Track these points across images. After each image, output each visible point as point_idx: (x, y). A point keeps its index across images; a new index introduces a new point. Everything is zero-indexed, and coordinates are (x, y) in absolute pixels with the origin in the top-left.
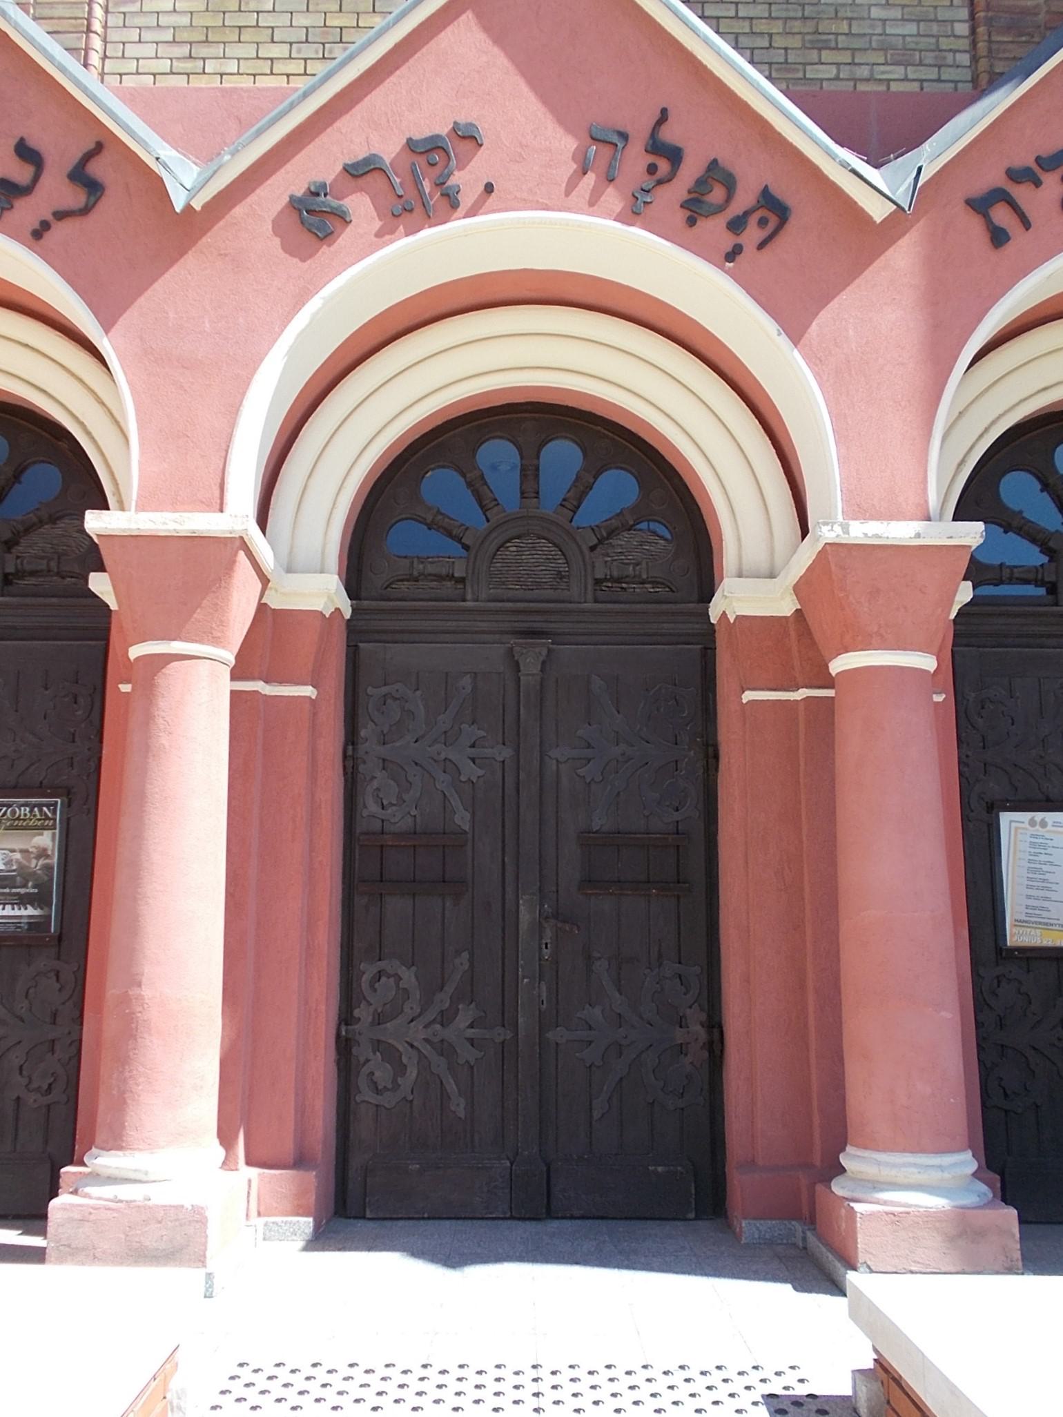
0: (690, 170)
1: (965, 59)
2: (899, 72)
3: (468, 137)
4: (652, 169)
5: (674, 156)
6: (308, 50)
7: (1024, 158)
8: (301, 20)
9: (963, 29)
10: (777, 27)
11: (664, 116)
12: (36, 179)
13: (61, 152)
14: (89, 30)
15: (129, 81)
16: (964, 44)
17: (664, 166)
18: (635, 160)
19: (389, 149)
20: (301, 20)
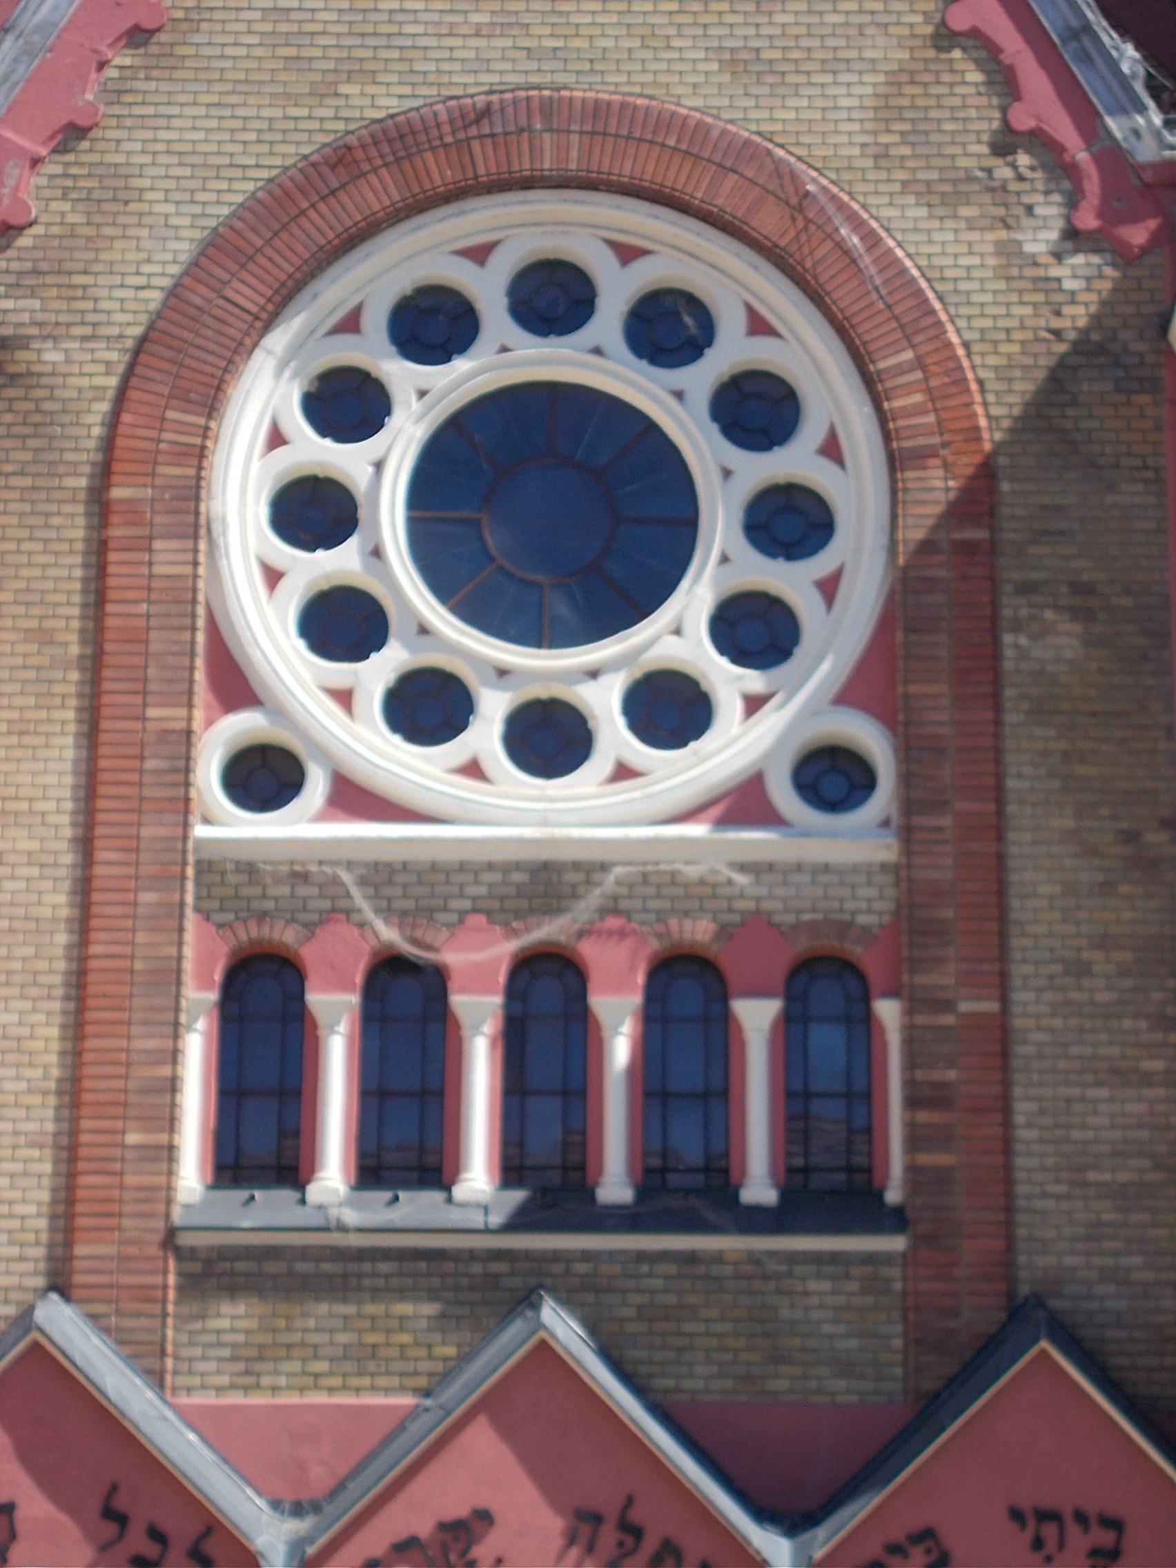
0: (650, 1545)
1: (898, 1371)
2: (842, 1384)
3: (484, 1517)
4: (621, 1544)
5: (637, 1533)
6: (349, 1366)
7: (897, 1534)
8: (343, 1338)
9: (898, 1343)
10: (742, 1343)
11: (629, 1501)
12: (162, 1555)
13: (182, 1532)
14: (163, 1353)
15: (198, 1399)
16: (899, 1357)
17: (629, 1541)
18: (609, 1536)
19: (423, 1528)
20: (343, 1338)
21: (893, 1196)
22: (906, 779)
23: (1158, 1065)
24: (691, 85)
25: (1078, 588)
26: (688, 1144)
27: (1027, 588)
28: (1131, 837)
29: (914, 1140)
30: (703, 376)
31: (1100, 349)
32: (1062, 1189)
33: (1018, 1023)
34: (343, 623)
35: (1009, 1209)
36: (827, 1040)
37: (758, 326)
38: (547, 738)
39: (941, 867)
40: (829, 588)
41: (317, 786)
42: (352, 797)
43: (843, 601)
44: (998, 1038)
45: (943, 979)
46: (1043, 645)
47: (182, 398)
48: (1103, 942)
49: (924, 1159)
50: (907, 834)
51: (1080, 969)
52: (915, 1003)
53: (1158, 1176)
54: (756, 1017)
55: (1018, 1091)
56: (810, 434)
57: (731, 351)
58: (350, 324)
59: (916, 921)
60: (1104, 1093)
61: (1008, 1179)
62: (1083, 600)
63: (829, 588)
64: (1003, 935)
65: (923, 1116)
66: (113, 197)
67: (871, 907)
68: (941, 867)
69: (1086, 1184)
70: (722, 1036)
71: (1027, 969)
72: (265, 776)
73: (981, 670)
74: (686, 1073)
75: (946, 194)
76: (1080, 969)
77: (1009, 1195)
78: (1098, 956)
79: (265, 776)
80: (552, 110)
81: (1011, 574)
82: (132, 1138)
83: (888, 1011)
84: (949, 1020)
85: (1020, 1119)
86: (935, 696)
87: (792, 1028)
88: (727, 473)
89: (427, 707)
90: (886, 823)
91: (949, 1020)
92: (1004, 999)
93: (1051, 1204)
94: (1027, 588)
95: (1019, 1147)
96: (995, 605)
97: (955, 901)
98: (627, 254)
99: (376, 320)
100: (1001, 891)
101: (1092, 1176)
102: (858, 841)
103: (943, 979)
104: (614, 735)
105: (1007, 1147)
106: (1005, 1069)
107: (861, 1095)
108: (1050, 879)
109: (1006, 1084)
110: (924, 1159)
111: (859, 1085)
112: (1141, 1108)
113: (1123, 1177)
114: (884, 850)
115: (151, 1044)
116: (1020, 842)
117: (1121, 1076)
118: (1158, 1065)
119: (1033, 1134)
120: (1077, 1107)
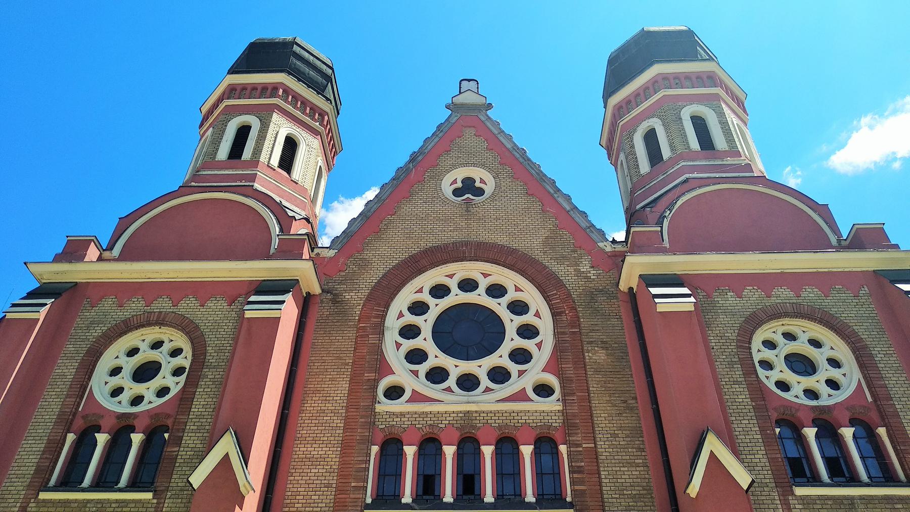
21: (569, 499)
22: (563, 387)
23: (641, 461)
24: (501, 239)
25: (605, 343)
26: (509, 489)
27: (591, 343)
28: (625, 402)
29: (573, 483)
30: (505, 300)
31: (602, 290)
32: (617, 496)
33: (600, 450)
34: (415, 357)
35: (603, 502)
36: (546, 459)
37: (517, 289)
38: (468, 383)
39: (575, 409)
40: (539, 346)
41: (407, 395)
42: (417, 397)
43: (542, 349)
44: (594, 454)
45: (578, 438)
46: (597, 356)
47: (379, 305)
48: (621, 428)
49: (577, 487)
50: (564, 401)
51: (615, 436)
52: (570, 445)
53: (645, 492)
54: (527, 451)
55: (602, 469)
56: (532, 311)
57: (511, 295)
58: (420, 291)
59: (569, 424)
60: (626, 469)
61: (602, 494)
62: (605, 345)
63: (539, 346)
64: (593, 427)
65: (575, 476)
66: (364, 265)
67: (557, 422)
68: (575, 409)
69: (624, 494)
70: (517, 455)
71: (601, 436)
72: (394, 392)
73: (580, 362)
74: (508, 469)
75: (561, 259)
76: (615, 436)
77: (602, 498)
78: (620, 432)
79: (394, 392)
80: (466, 244)
81: (584, 339)
82: (353, 484)
83: (563, 448)
84: (581, 449)
85: (603, 477)
86: (569, 369)
87: (537, 454)
88: (512, 321)
89: (437, 375)
90: (558, 400)
91: (581, 449)
92: (595, 443)
93: (614, 500)
94: (591, 343)
95: (604, 484)
96: (583, 347)
97: (577, 419)
98: (485, 275)
99: (426, 290)
100: (591, 416)
101: (625, 492)
102: (552, 405)
103: (578, 438)
104: (485, 382)
105: (600, 484)
106: (597, 462)
107: (557, 474)
108: (604, 415)
109: (598, 467)
110: (577, 487)
111: (556, 471)
112: (638, 473)
113: (634, 492)
114: (559, 407)
115: (360, 459)
116: (595, 402)
117: (632, 464)
118: (641, 461)
119: (607, 481)
120: (618, 473)
